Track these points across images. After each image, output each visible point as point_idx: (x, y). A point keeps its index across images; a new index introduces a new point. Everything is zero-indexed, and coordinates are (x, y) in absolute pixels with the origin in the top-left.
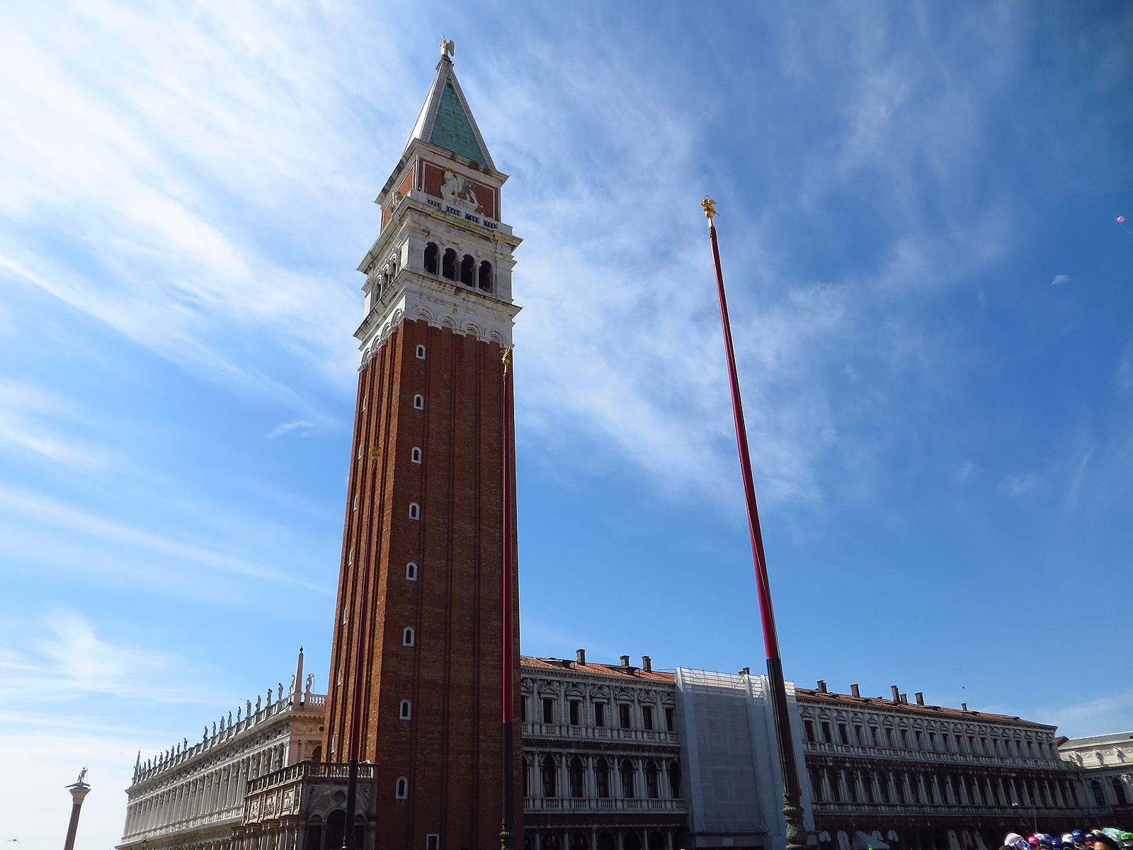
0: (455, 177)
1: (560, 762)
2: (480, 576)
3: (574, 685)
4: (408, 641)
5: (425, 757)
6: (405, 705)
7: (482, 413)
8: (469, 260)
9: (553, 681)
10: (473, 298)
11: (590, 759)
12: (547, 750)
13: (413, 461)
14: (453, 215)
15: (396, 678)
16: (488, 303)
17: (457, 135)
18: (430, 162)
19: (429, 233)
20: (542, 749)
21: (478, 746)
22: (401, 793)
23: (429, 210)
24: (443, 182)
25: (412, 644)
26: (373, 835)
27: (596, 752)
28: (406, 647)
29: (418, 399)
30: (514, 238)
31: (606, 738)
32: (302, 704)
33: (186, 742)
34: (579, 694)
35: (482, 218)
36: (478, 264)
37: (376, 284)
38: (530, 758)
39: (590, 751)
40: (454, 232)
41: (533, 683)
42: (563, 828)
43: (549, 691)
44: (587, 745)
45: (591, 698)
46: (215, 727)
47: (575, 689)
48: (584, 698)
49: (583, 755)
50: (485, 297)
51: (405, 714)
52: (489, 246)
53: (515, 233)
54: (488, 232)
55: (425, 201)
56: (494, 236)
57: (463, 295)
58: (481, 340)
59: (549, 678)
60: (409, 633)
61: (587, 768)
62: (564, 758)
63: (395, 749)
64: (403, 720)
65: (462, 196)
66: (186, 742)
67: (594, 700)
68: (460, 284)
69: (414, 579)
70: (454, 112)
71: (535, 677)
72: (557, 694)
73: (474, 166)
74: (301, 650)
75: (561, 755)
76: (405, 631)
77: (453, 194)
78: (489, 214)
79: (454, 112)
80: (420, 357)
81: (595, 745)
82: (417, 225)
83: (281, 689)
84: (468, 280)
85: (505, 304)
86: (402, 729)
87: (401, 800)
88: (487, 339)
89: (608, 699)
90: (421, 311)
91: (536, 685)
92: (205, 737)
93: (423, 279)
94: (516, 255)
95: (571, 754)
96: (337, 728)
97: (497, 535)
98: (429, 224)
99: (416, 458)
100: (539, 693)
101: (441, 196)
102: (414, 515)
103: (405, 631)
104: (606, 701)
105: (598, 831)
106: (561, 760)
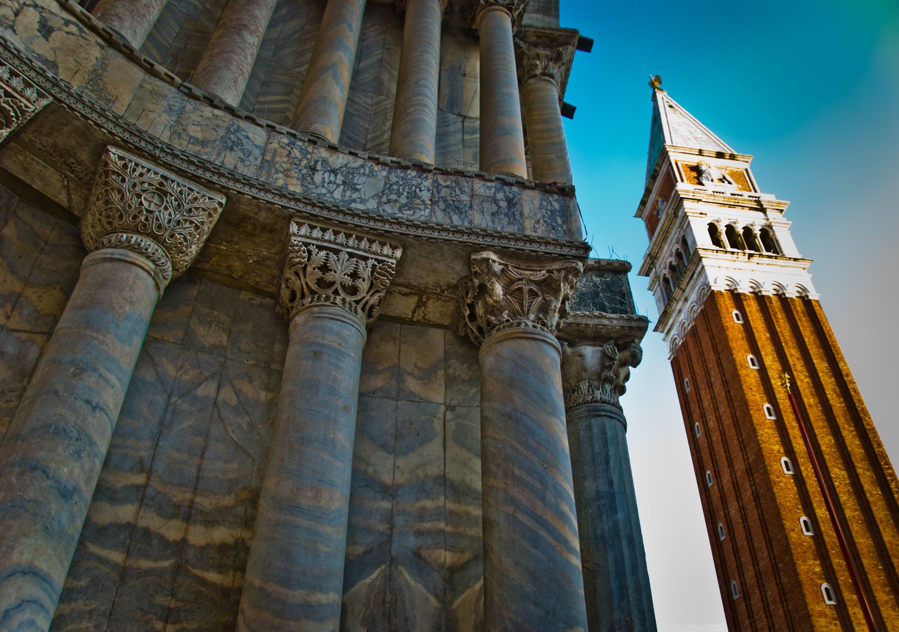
8: (748, 230)
17: (695, 138)
36: (757, 232)
57: (756, 259)
68: (747, 251)
84: (753, 246)
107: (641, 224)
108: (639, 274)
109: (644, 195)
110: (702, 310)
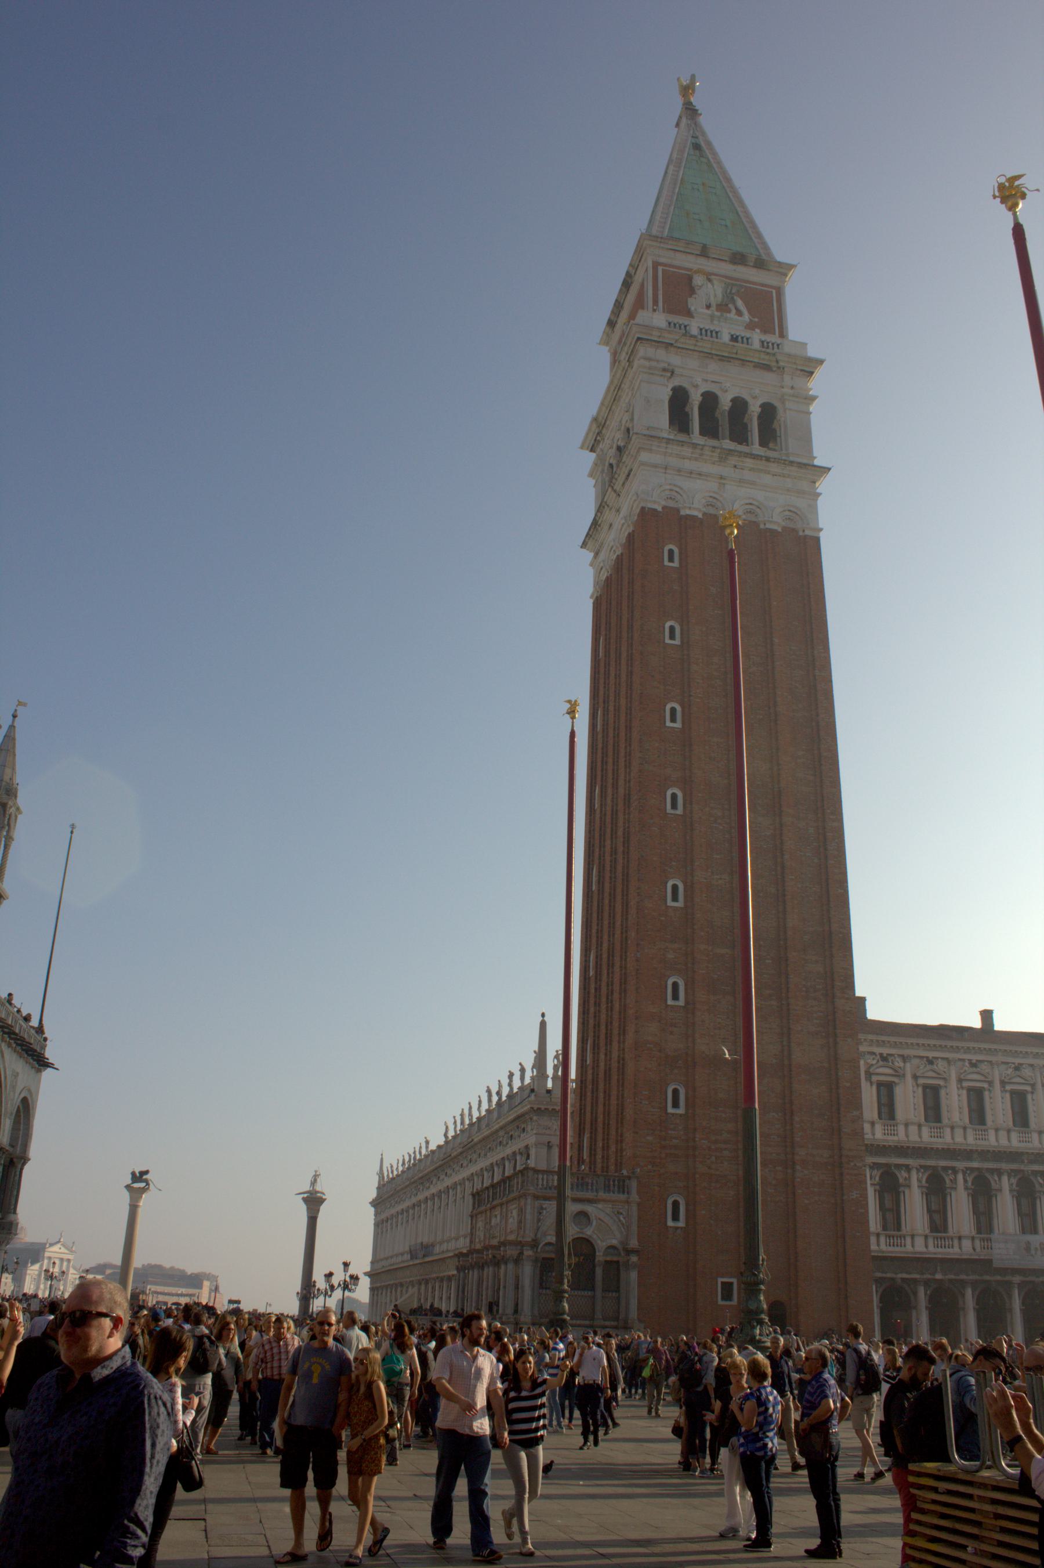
0: (710, 280)
1: (954, 1181)
2: (784, 895)
3: (973, 1065)
4: (675, 997)
5: (709, 1168)
6: (675, 1092)
7: (776, 640)
8: (739, 406)
9: (937, 1058)
10: (749, 462)
11: (1005, 1178)
12: (931, 1163)
13: (669, 724)
14: (708, 338)
15: (660, 1051)
16: (774, 468)
18: (670, 266)
19: (673, 373)
20: (923, 1162)
21: (793, 1154)
22: (676, 1217)
23: (669, 338)
24: (692, 291)
25: (681, 1002)
26: (634, 1275)
27: (1014, 1166)
28: (672, 1007)
29: (672, 629)
30: (810, 360)
31: (1030, 1145)
32: (549, 1092)
33: (427, 1142)
34: (982, 1078)
35: (756, 337)
36: (755, 409)
37: (607, 464)
38: (905, 1174)
39: (1004, 1166)
40: (713, 366)
41: (905, 1062)
42: (962, 1280)
43: (931, 1074)
44: (998, 1155)
45: (1003, 1083)
46: (455, 1122)
47: (974, 1069)
48: (991, 1083)
49: (992, 1171)
50: (768, 459)
51: (676, 1105)
52: (769, 377)
53: (812, 352)
54: (767, 357)
55: (663, 324)
56: (777, 362)
57: (733, 460)
58: (768, 526)
59: (931, 1054)
60: (675, 985)
61: (1000, 1190)
62: (960, 1177)
63: (663, 1155)
64: (673, 1114)
65: (722, 307)
66: (427, 1142)
67: (1008, 1087)
68: (728, 444)
69: (680, 904)
70: (703, 184)
71: (907, 1052)
72: (945, 1079)
73: (738, 259)
74: (543, 1015)
75: (955, 1171)
76: (670, 982)
77: (708, 307)
78: (767, 330)
79: (703, 184)
80: (671, 564)
81: (1014, 1156)
82: (654, 364)
83: (523, 1070)
84: (740, 435)
85: (802, 466)
86: (672, 1126)
87: (677, 1228)
88: (775, 521)
89: (1033, 1086)
90: (667, 492)
91: (908, 1065)
92: (446, 1135)
93: (667, 443)
94: (816, 385)
95: (972, 1170)
96: (588, 1126)
97: (811, 830)
98: (675, 360)
99: (673, 719)
100: (915, 1077)
101: (689, 314)
102: (674, 806)
103: (670, 982)
104: (1028, 1088)
105: (1020, 1285)
106: (955, 1179)
107: (604, 355)
108: (582, 448)
109: (613, 312)
110: (629, 534)
